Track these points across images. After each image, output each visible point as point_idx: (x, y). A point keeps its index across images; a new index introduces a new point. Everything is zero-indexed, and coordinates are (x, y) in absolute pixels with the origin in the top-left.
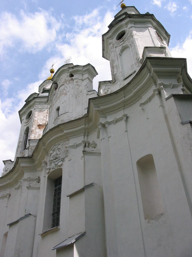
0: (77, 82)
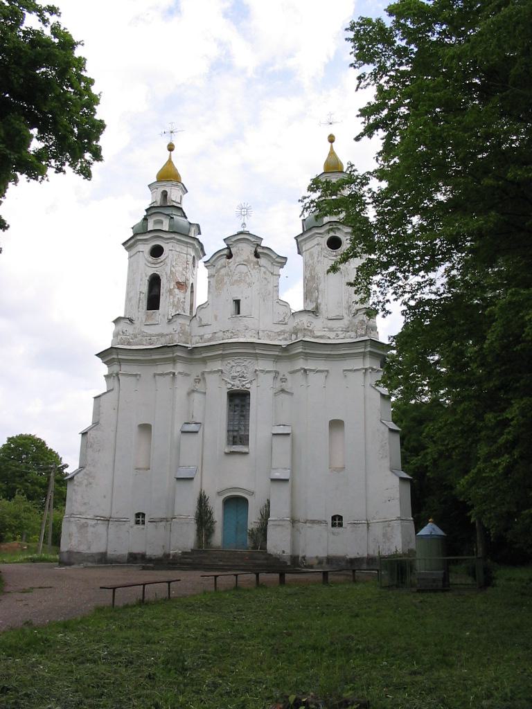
0: (265, 273)
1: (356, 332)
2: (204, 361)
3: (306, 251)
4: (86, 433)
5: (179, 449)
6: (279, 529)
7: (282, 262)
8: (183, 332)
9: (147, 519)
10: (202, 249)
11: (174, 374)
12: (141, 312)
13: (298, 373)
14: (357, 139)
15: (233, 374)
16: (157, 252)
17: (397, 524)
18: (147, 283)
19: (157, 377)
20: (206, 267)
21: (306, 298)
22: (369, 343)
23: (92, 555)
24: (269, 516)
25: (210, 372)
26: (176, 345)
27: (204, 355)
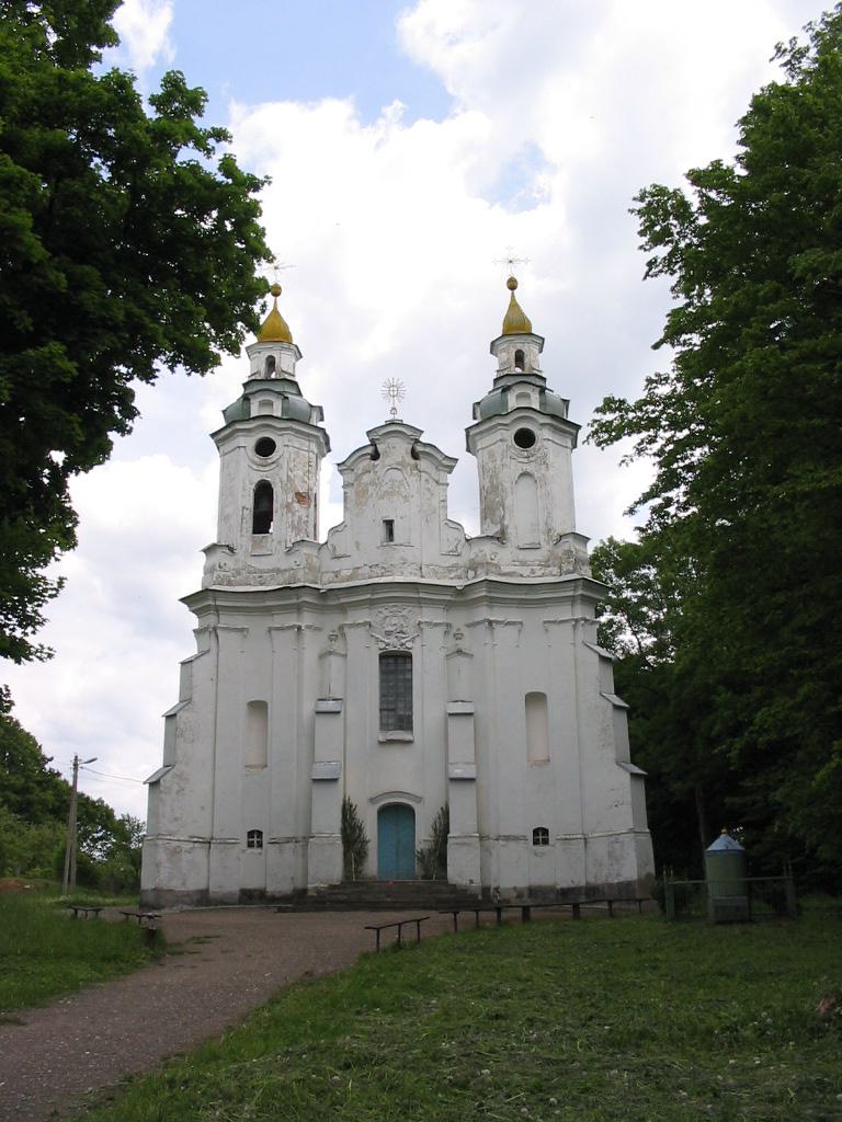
0: (427, 480)
1: (560, 568)
2: (343, 608)
3: (483, 449)
4: (175, 715)
5: (312, 737)
6: (465, 848)
7: (449, 464)
8: (310, 567)
9: (265, 839)
10: (327, 443)
11: (299, 628)
12: (243, 536)
13: (479, 626)
14: (656, 346)
15: (388, 629)
16: (265, 448)
17: (629, 840)
18: (252, 494)
19: (273, 632)
20: (340, 471)
21: (484, 518)
22: (581, 583)
23: (188, 894)
24: (448, 832)
25: (352, 626)
26: (304, 587)
27: (342, 601)
